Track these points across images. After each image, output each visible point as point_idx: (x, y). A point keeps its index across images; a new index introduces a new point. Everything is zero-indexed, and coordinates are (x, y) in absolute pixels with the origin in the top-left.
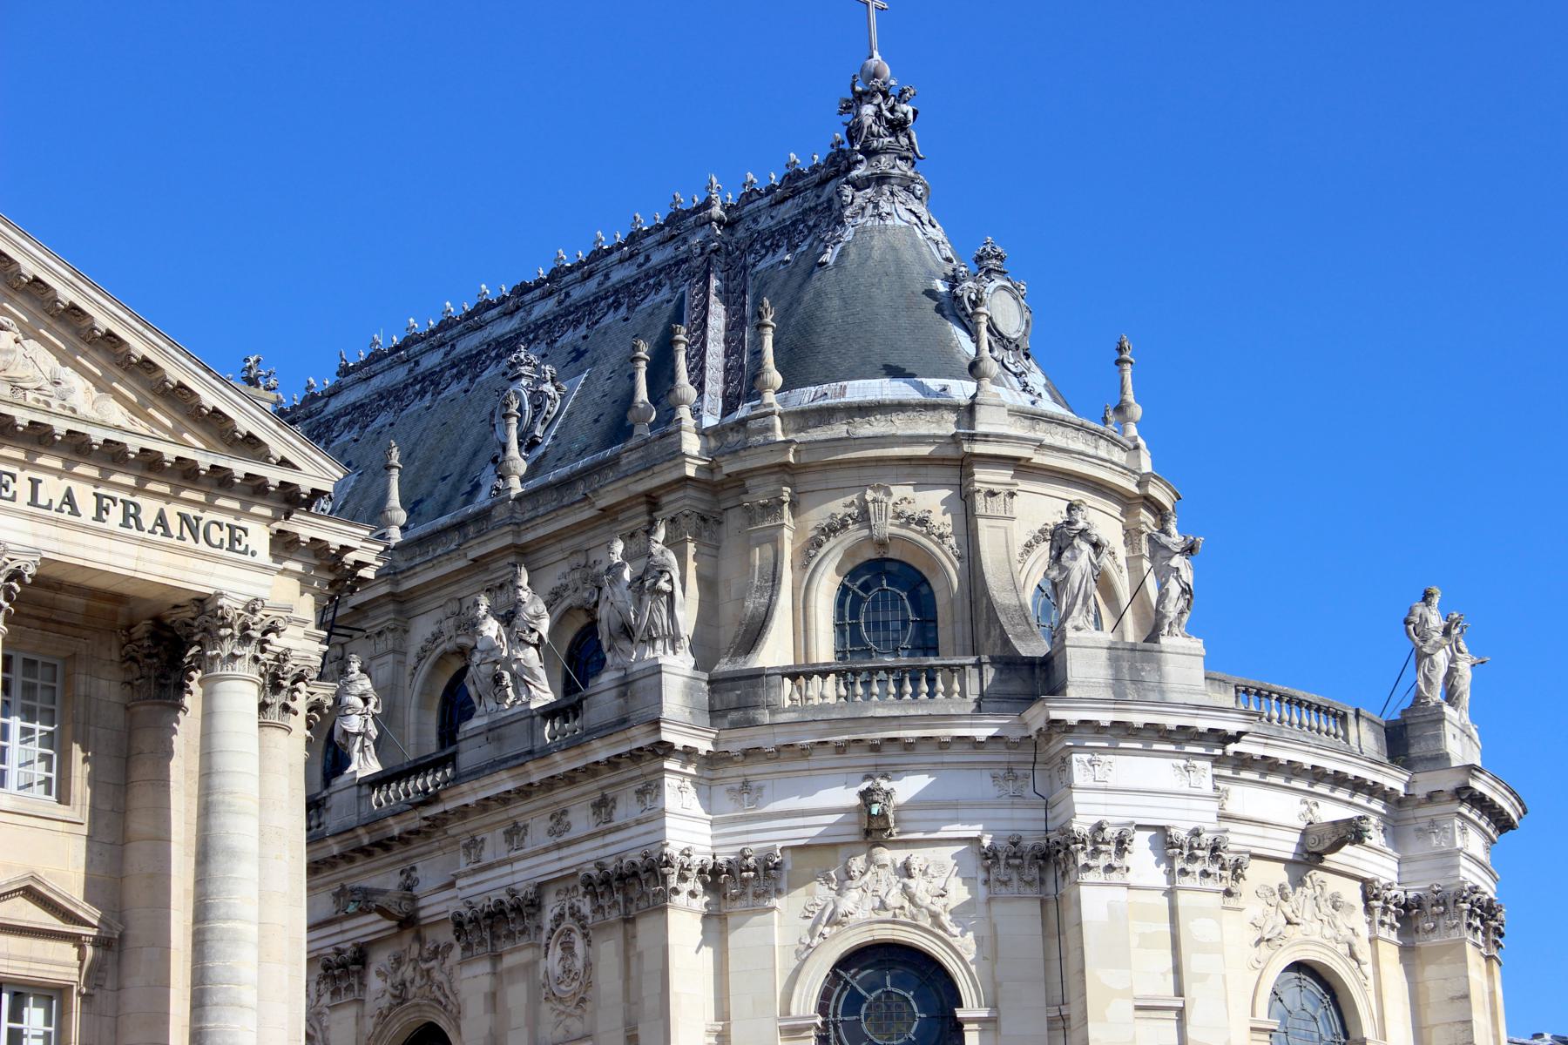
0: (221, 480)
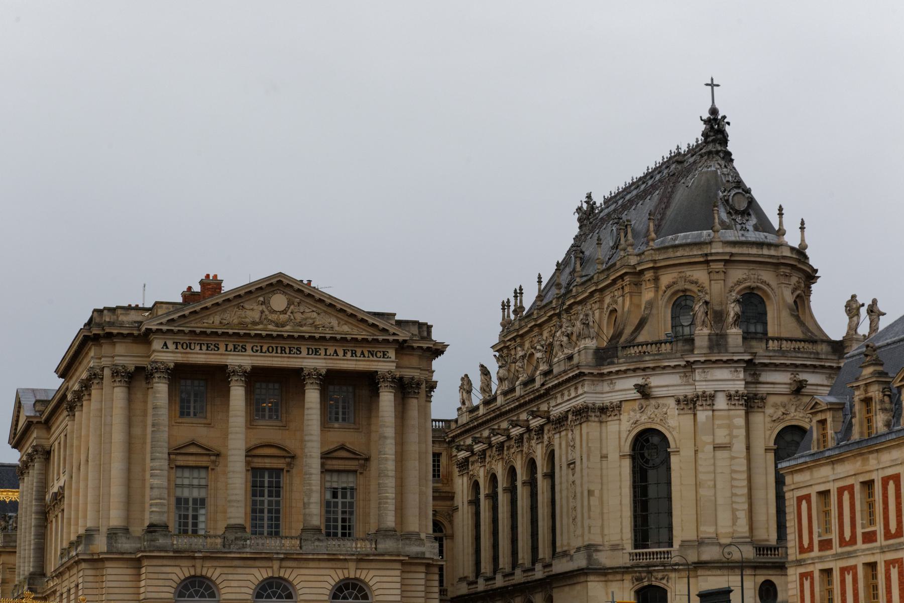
0: (376, 341)
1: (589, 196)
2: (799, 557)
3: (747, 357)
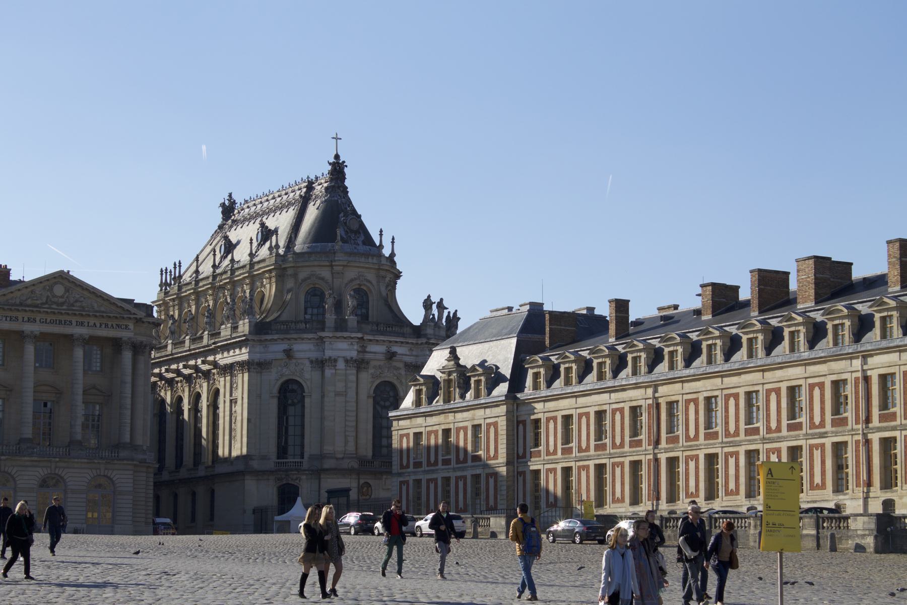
1: (230, 195)
2: (400, 471)
3: (360, 335)
